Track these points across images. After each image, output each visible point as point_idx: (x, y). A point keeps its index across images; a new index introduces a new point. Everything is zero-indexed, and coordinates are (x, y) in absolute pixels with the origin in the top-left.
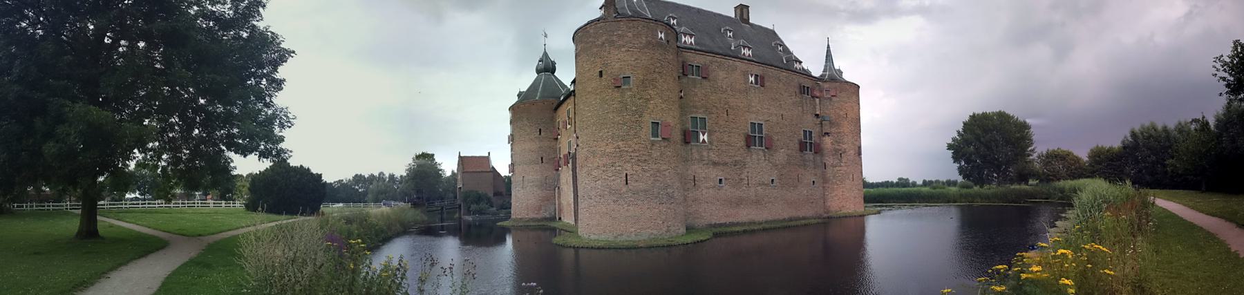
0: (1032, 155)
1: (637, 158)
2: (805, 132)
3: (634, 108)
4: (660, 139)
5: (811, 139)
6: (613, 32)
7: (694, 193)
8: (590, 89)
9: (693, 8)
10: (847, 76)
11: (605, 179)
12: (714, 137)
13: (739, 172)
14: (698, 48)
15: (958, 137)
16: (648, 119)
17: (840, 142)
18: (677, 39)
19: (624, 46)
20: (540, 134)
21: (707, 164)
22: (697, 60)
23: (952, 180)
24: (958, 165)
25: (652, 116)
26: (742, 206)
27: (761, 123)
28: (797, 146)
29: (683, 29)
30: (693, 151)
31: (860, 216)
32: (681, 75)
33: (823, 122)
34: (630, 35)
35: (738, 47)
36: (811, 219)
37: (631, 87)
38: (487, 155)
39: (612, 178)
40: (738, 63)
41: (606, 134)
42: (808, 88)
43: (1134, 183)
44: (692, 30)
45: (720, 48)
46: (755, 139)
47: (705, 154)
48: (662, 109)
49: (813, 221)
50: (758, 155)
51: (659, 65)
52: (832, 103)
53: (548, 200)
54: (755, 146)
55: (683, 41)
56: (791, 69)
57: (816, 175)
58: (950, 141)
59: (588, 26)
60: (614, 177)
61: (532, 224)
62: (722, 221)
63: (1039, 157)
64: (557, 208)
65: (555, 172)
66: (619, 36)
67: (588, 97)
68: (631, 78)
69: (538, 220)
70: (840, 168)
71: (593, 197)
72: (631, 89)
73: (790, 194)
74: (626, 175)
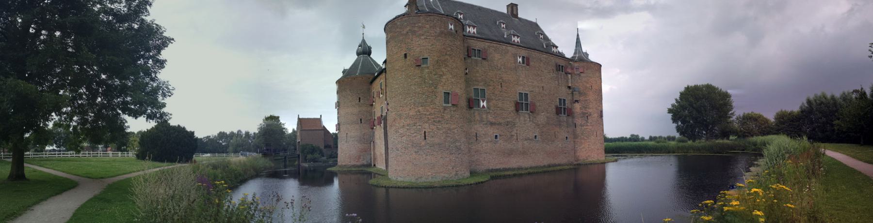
0: (732, 117)
1: (432, 120)
2: (560, 100)
3: (430, 82)
4: (450, 105)
6: (415, 24)
7: (476, 146)
8: (397, 68)
9: (476, 6)
10: (592, 58)
12: (491, 104)
13: (510, 130)
14: (479, 36)
15: (676, 104)
16: (441, 90)
17: (586, 108)
18: (463, 29)
19: (423, 35)
20: (360, 101)
21: (486, 124)
22: (478, 45)
23: (671, 136)
24: (676, 125)
27: (527, 92)
28: (554, 110)
29: (467, 22)
31: (602, 163)
32: (467, 57)
33: (574, 92)
34: (428, 26)
35: (510, 35)
36: (565, 165)
37: (428, 65)
38: (319, 117)
39: (414, 135)
40: (510, 48)
41: (410, 102)
42: (562, 66)
43: (809, 139)
44: (475, 22)
45: (496, 36)
46: (522, 105)
47: (484, 116)
49: (566, 167)
52: (581, 78)
53: (366, 151)
54: (523, 110)
55: (468, 31)
56: (550, 52)
58: (670, 107)
59: (396, 19)
61: (353, 169)
62: (498, 167)
63: (737, 119)
64: (372, 157)
65: (370, 130)
66: (420, 27)
67: (396, 73)
70: (586, 127)
71: (400, 149)
72: (428, 68)
73: (548, 147)
74: (425, 132)
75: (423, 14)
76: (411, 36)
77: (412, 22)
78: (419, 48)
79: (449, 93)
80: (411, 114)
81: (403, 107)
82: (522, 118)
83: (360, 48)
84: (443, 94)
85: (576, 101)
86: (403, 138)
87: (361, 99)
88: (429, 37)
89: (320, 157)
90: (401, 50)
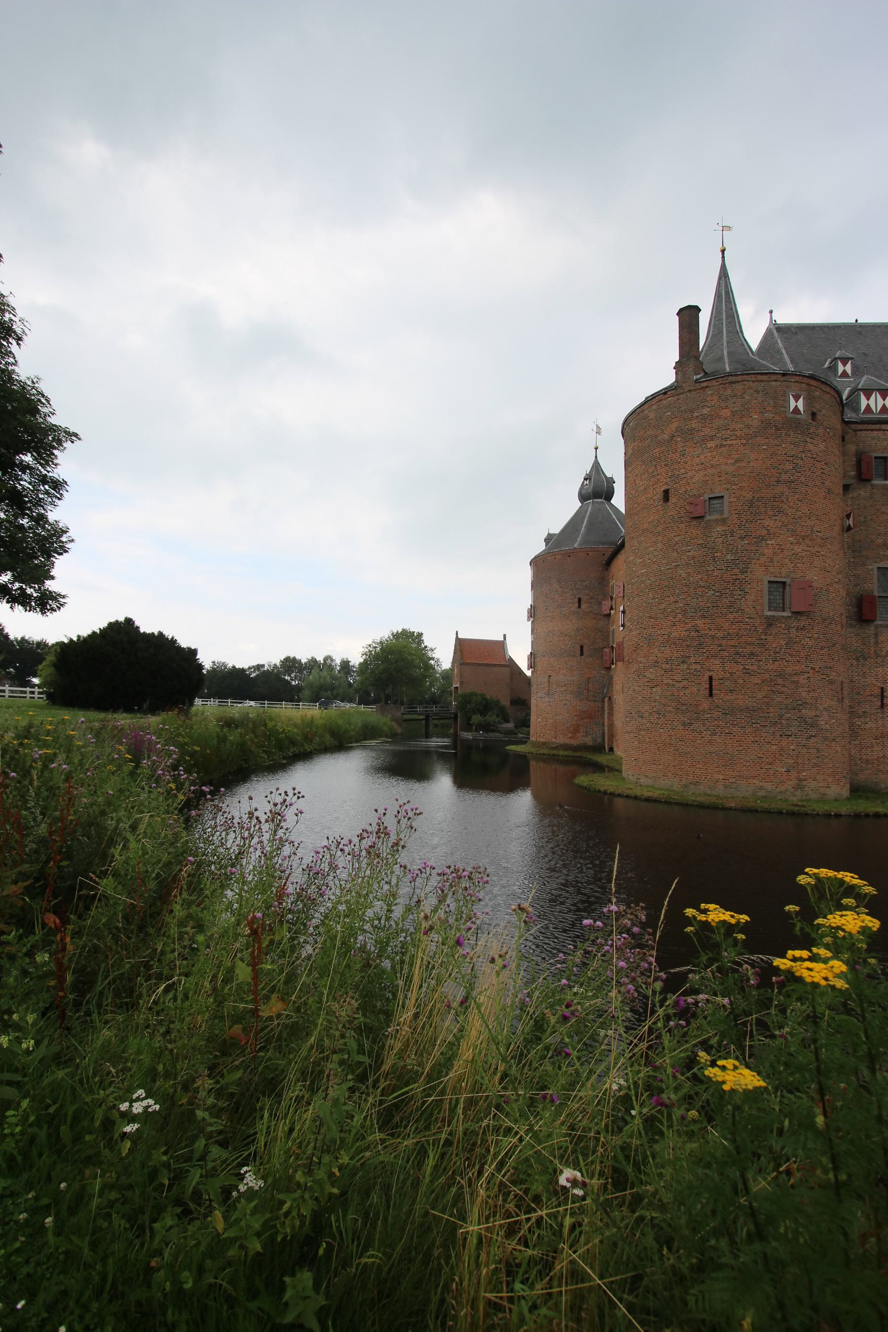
3: (729, 557)
8: (646, 526)
11: (668, 684)
25: (771, 569)
39: (681, 685)
59: (646, 406)
60: (685, 683)
71: (646, 715)
72: (724, 521)
74: (711, 678)
79: (784, 583)
80: (675, 634)
81: (656, 619)
86: (654, 690)
89: (500, 723)
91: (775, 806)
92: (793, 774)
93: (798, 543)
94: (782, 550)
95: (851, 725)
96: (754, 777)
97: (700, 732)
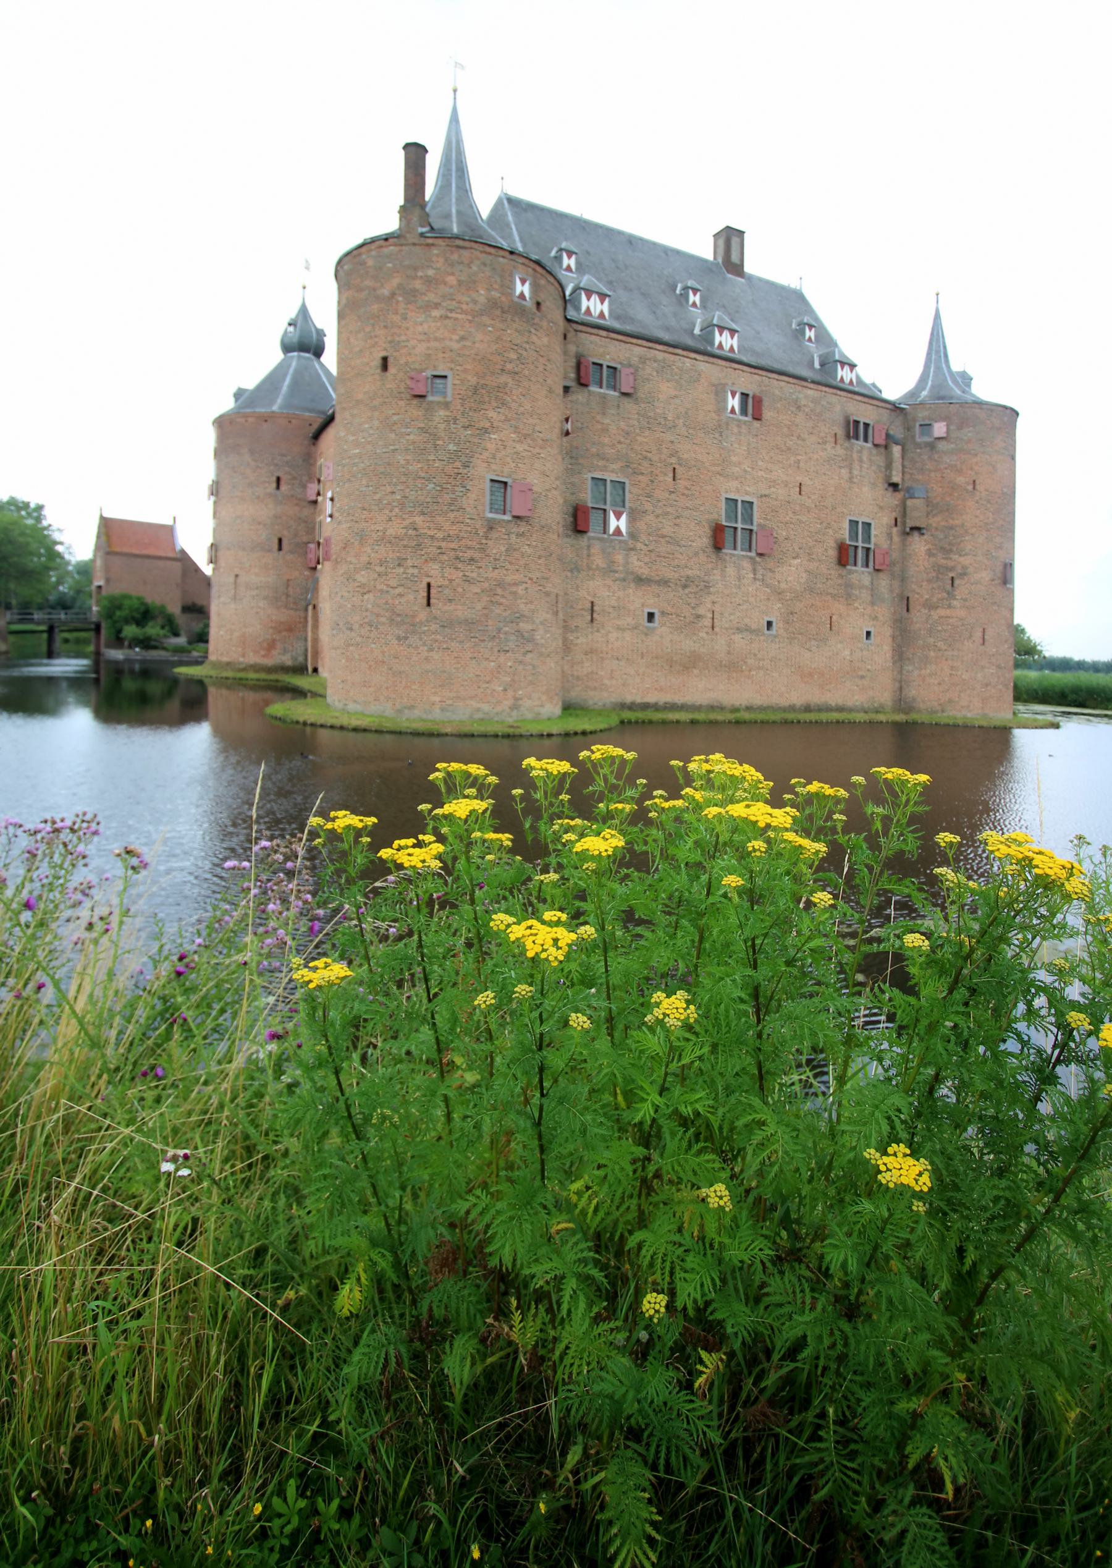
1: (452, 553)
2: (854, 524)
3: (451, 447)
5: (867, 538)
11: (381, 591)
13: (693, 601)
16: (483, 473)
19: (437, 306)
25: (494, 467)
26: (696, 671)
28: (833, 553)
30: (593, 551)
33: (909, 503)
36: (858, 711)
37: (449, 399)
39: (397, 591)
48: (517, 453)
49: (860, 717)
50: (739, 568)
51: (513, 356)
54: (735, 548)
57: (875, 618)
60: (400, 590)
65: (307, 573)
66: (428, 281)
67: (355, 412)
68: (450, 378)
69: (269, 670)
72: (446, 405)
74: (429, 585)
75: (440, 242)
76: (402, 306)
77: (407, 263)
78: (425, 345)
79: (505, 483)
82: (731, 571)
83: (291, 329)
84: (488, 484)
85: (912, 529)
87: (282, 483)
88: (453, 315)
90: (373, 346)
91: (491, 729)
92: (510, 693)
93: (520, 442)
94: (505, 447)
95: (565, 640)
96: (472, 698)
97: (417, 648)
